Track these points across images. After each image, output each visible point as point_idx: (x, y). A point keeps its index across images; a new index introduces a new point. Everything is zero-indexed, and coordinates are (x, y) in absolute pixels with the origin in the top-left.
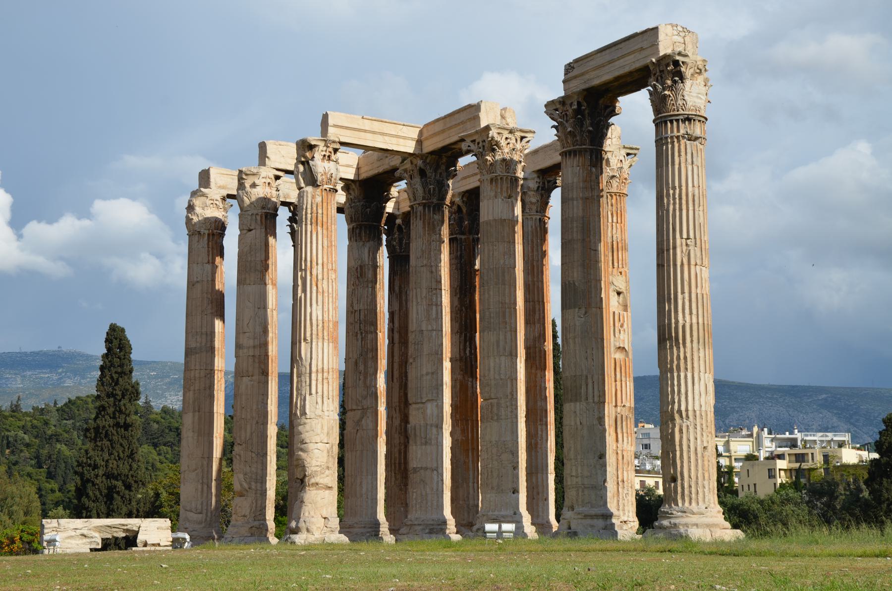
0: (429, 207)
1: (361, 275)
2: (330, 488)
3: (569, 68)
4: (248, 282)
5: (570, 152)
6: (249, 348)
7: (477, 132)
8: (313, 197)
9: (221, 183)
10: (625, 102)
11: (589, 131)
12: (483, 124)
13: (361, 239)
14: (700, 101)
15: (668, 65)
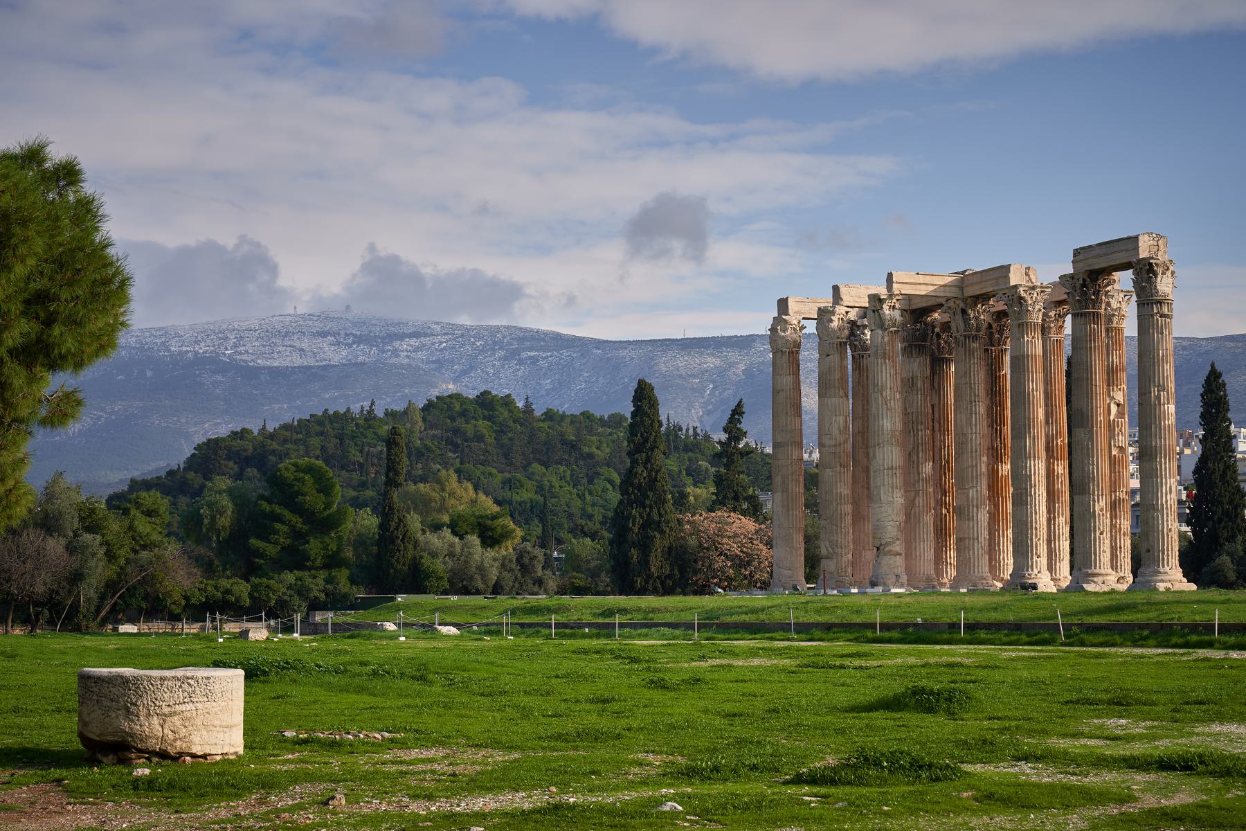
0: (969, 338)
1: (913, 384)
2: (900, 554)
3: (1077, 253)
4: (828, 395)
5: (1078, 314)
6: (829, 446)
7: (1007, 288)
8: (883, 338)
9: (796, 309)
10: (1117, 275)
11: (1092, 299)
12: (1012, 283)
13: (912, 356)
14: (1168, 289)
15: (1144, 265)
